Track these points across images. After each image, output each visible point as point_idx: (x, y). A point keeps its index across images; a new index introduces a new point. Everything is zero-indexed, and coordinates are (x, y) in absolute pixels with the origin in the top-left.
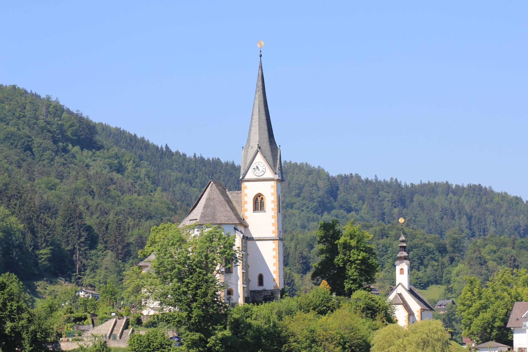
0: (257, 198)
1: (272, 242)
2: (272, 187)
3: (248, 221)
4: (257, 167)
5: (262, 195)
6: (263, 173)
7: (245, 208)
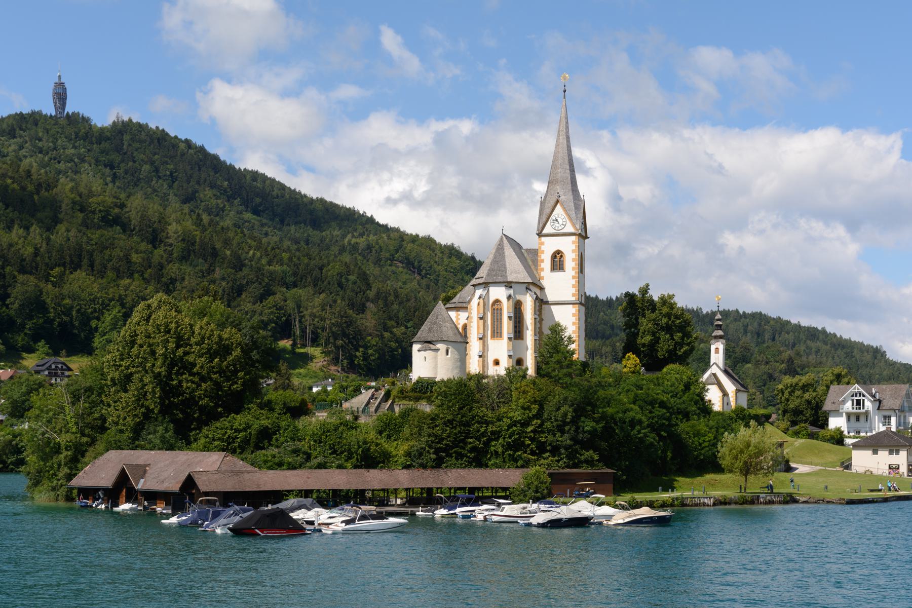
0: (556, 256)
1: (571, 306)
2: (573, 242)
3: (544, 283)
4: (557, 220)
5: (562, 252)
6: (563, 226)
7: (542, 267)
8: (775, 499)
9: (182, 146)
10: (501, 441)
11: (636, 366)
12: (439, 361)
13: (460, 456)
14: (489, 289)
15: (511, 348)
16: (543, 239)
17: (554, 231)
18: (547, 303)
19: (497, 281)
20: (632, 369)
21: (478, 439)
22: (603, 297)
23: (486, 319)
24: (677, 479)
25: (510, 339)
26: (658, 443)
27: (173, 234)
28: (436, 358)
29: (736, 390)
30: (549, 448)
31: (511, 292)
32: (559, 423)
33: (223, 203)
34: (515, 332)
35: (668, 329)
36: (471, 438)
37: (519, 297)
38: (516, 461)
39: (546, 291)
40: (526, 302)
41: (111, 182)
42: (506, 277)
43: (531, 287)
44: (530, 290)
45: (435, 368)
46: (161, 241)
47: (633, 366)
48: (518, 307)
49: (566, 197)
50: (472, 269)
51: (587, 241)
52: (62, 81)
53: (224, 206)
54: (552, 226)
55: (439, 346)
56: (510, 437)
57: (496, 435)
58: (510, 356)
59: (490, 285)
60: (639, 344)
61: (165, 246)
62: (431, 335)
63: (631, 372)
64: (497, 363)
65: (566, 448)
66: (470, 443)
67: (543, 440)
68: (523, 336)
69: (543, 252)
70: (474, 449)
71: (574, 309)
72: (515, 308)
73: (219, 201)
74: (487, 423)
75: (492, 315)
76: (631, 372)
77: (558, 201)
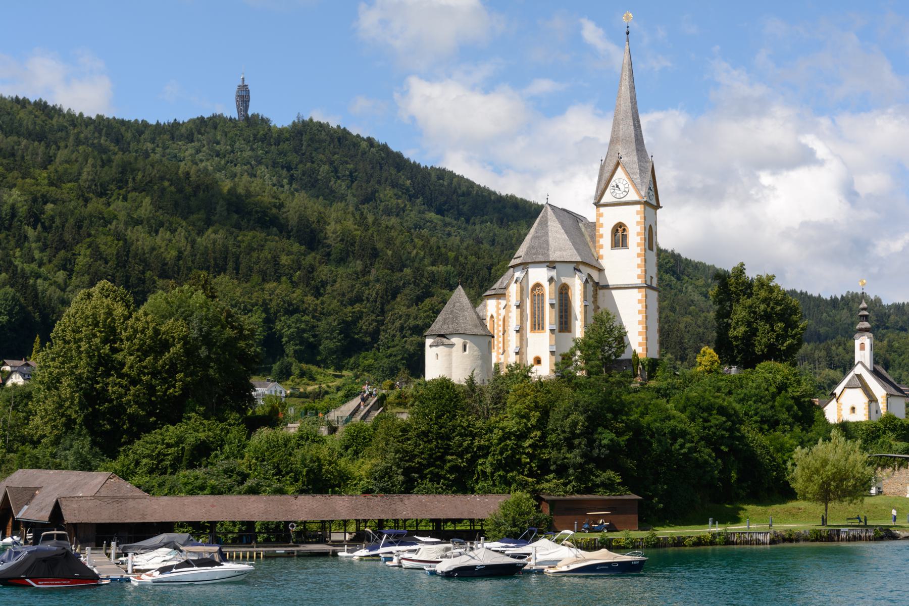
0: (617, 230)
1: (636, 290)
2: (638, 213)
3: (604, 263)
4: (617, 186)
5: (625, 225)
6: (625, 194)
7: (601, 243)
8: (863, 535)
9: (364, 145)
10: (490, 458)
11: (713, 364)
12: (454, 359)
13: (436, 478)
14: (527, 271)
15: (553, 343)
16: (602, 209)
17: (614, 200)
18: (607, 287)
19: (537, 260)
20: (708, 368)
21: (460, 456)
22: (826, 296)
23: (524, 308)
24: (745, 507)
25: (552, 331)
26: (715, 461)
27: (331, 235)
28: (450, 355)
29: (887, 394)
30: (553, 468)
31: (554, 273)
32: (567, 435)
33: (403, 202)
34: (561, 323)
35: (768, 317)
36: (452, 454)
37: (564, 280)
38: (509, 484)
39: (606, 272)
40: (574, 285)
41: (287, 184)
42: (548, 255)
43: (581, 267)
44: (579, 271)
45: (450, 367)
46: (319, 241)
47: (709, 364)
48: (563, 293)
49: (630, 158)
50: (672, 267)
51: (659, 211)
52: (246, 83)
53: (405, 206)
54: (612, 193)
55: (454, 340)
56: (501, 453)
57: (485, 451)
58: (552, 353)
59: (530, 265)
60: (732, 338)
61: (323, 247)
62: (445, 327)
63: (707, 371)
64: (538, 361)
65: (575, 467)
66: (449, 461)
67: (546, 456)
68: (572, 330)
69: (602, 225)
70: (454, 469)
71: (640, 294)
72: (561, 293)
73: (399, 201)
74: (473, 436)
75: (531, 302)
76: (707, 371)
77: (618, 164)
